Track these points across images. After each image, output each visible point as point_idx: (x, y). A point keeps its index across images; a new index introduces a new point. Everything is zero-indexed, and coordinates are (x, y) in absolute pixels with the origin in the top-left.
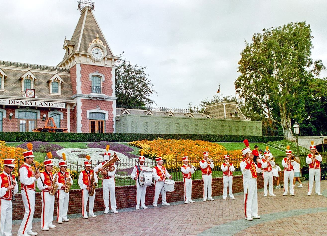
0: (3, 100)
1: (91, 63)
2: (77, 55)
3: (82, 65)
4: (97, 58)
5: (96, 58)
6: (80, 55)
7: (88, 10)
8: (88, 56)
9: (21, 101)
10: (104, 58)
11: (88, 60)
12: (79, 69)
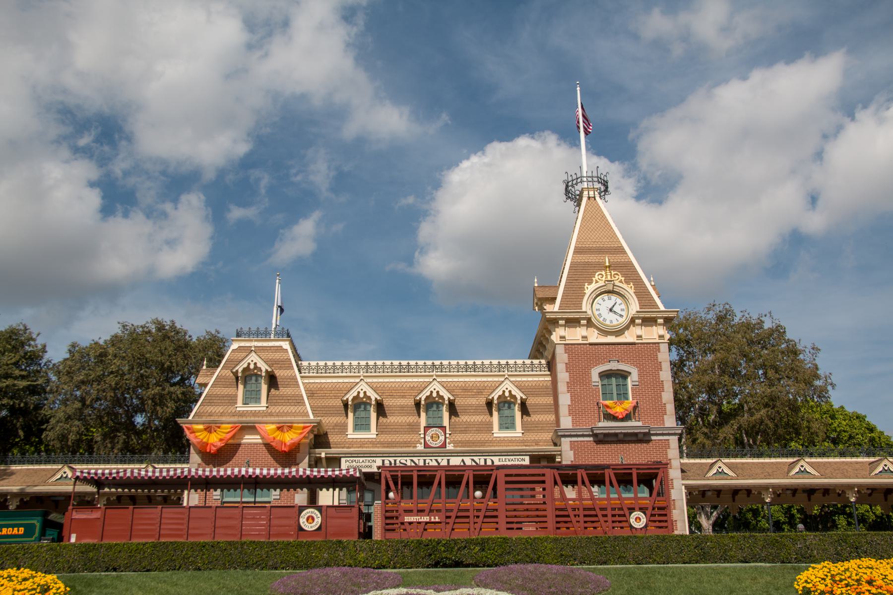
0: (369, 461)
1: (594, 337)
2: (554, 322)
3: (570, 348)
5: (608, 323)
6: (562, 322)
7: (589, 198)
9: (412, 460)
10: (632, 321)
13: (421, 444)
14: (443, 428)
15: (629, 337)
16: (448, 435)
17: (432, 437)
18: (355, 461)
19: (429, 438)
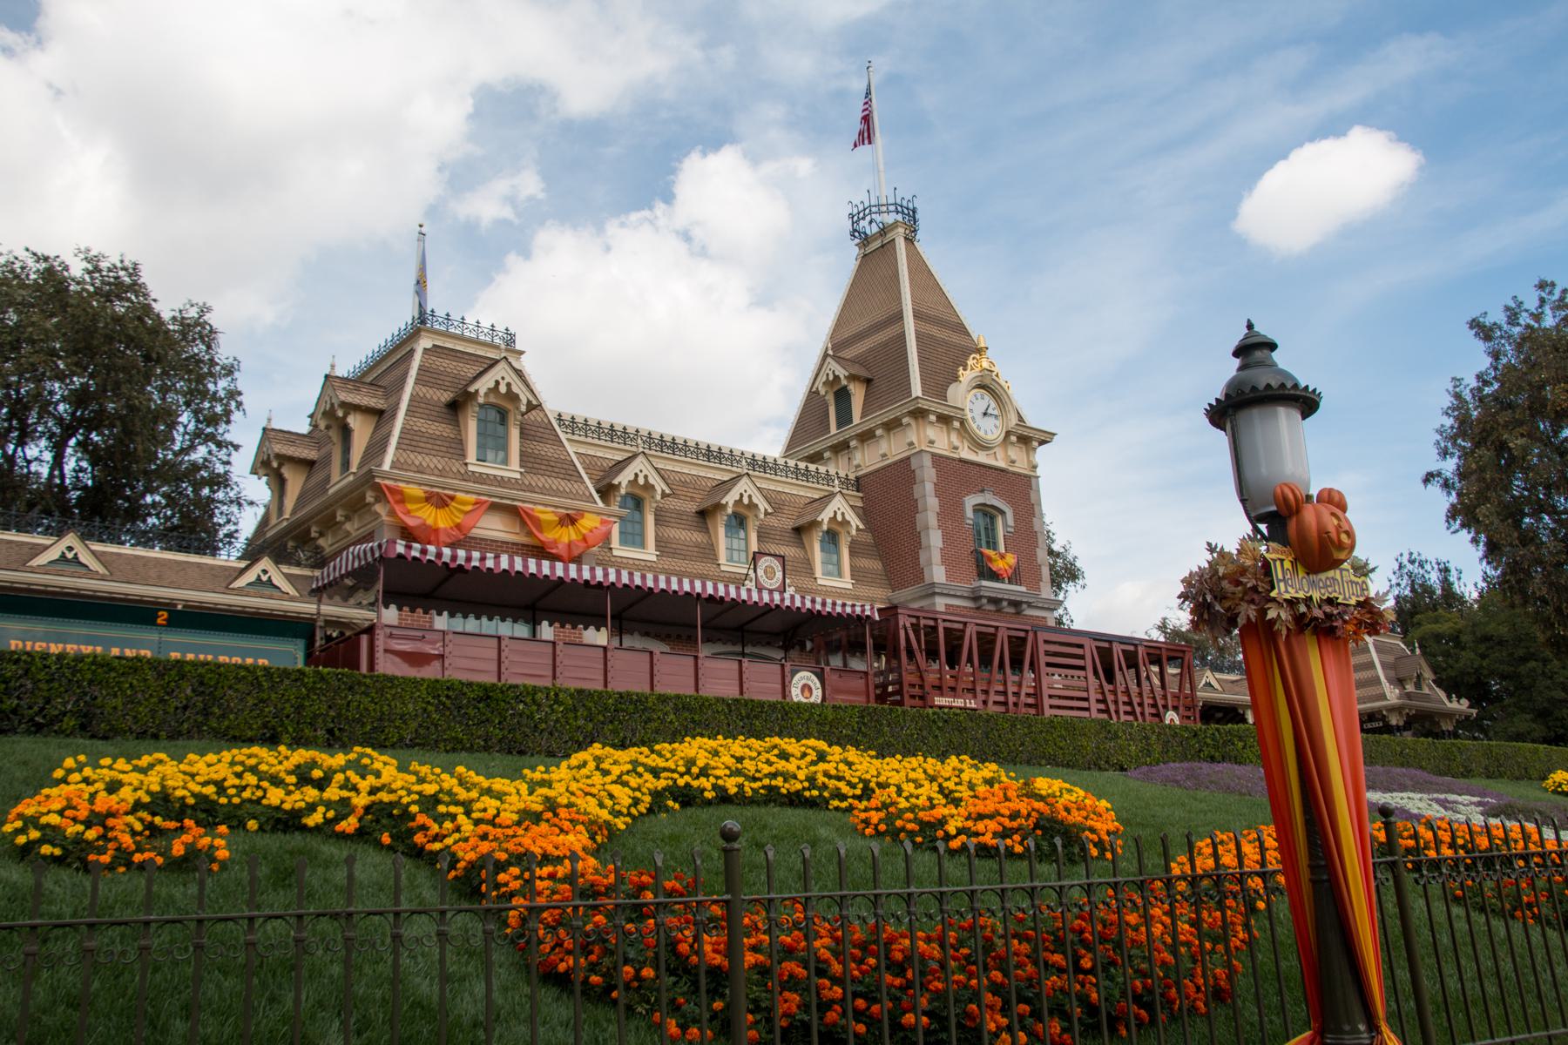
1: (966, 454)
3: (938, 459)
4: (986, 433)
8: (956, 424)
11: (954, 438)
12: (928, 476)
15: (1001, 464)
17: (766, 572)
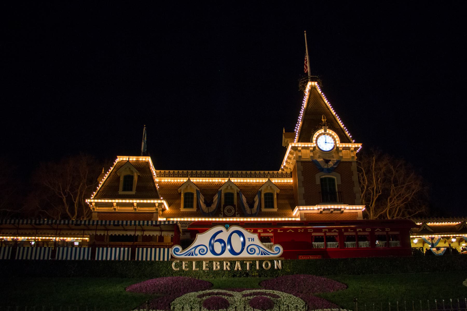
13: (221, 214)
14: (234, 206)
16: (236, 211)
17: (228, 211)
18: (185, 223)
19: (226, 211)
